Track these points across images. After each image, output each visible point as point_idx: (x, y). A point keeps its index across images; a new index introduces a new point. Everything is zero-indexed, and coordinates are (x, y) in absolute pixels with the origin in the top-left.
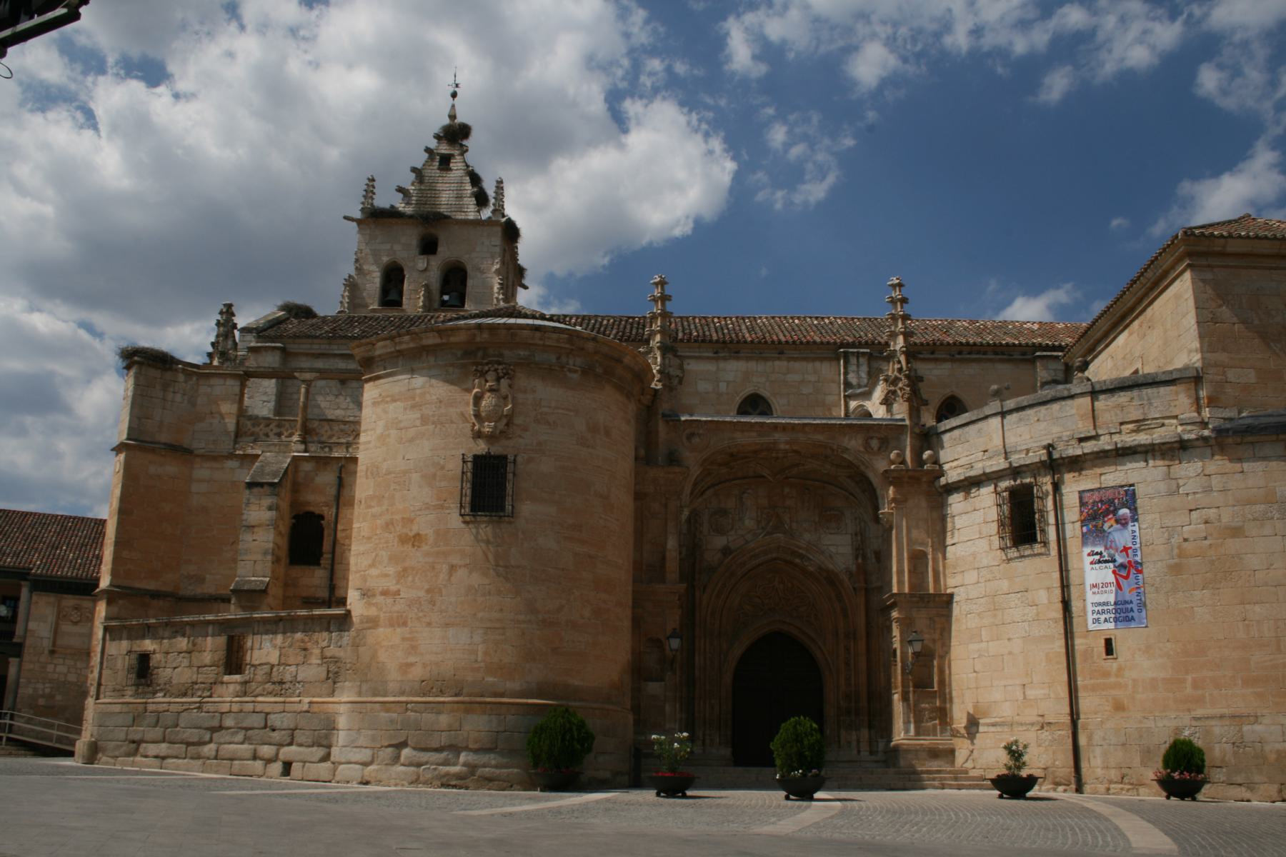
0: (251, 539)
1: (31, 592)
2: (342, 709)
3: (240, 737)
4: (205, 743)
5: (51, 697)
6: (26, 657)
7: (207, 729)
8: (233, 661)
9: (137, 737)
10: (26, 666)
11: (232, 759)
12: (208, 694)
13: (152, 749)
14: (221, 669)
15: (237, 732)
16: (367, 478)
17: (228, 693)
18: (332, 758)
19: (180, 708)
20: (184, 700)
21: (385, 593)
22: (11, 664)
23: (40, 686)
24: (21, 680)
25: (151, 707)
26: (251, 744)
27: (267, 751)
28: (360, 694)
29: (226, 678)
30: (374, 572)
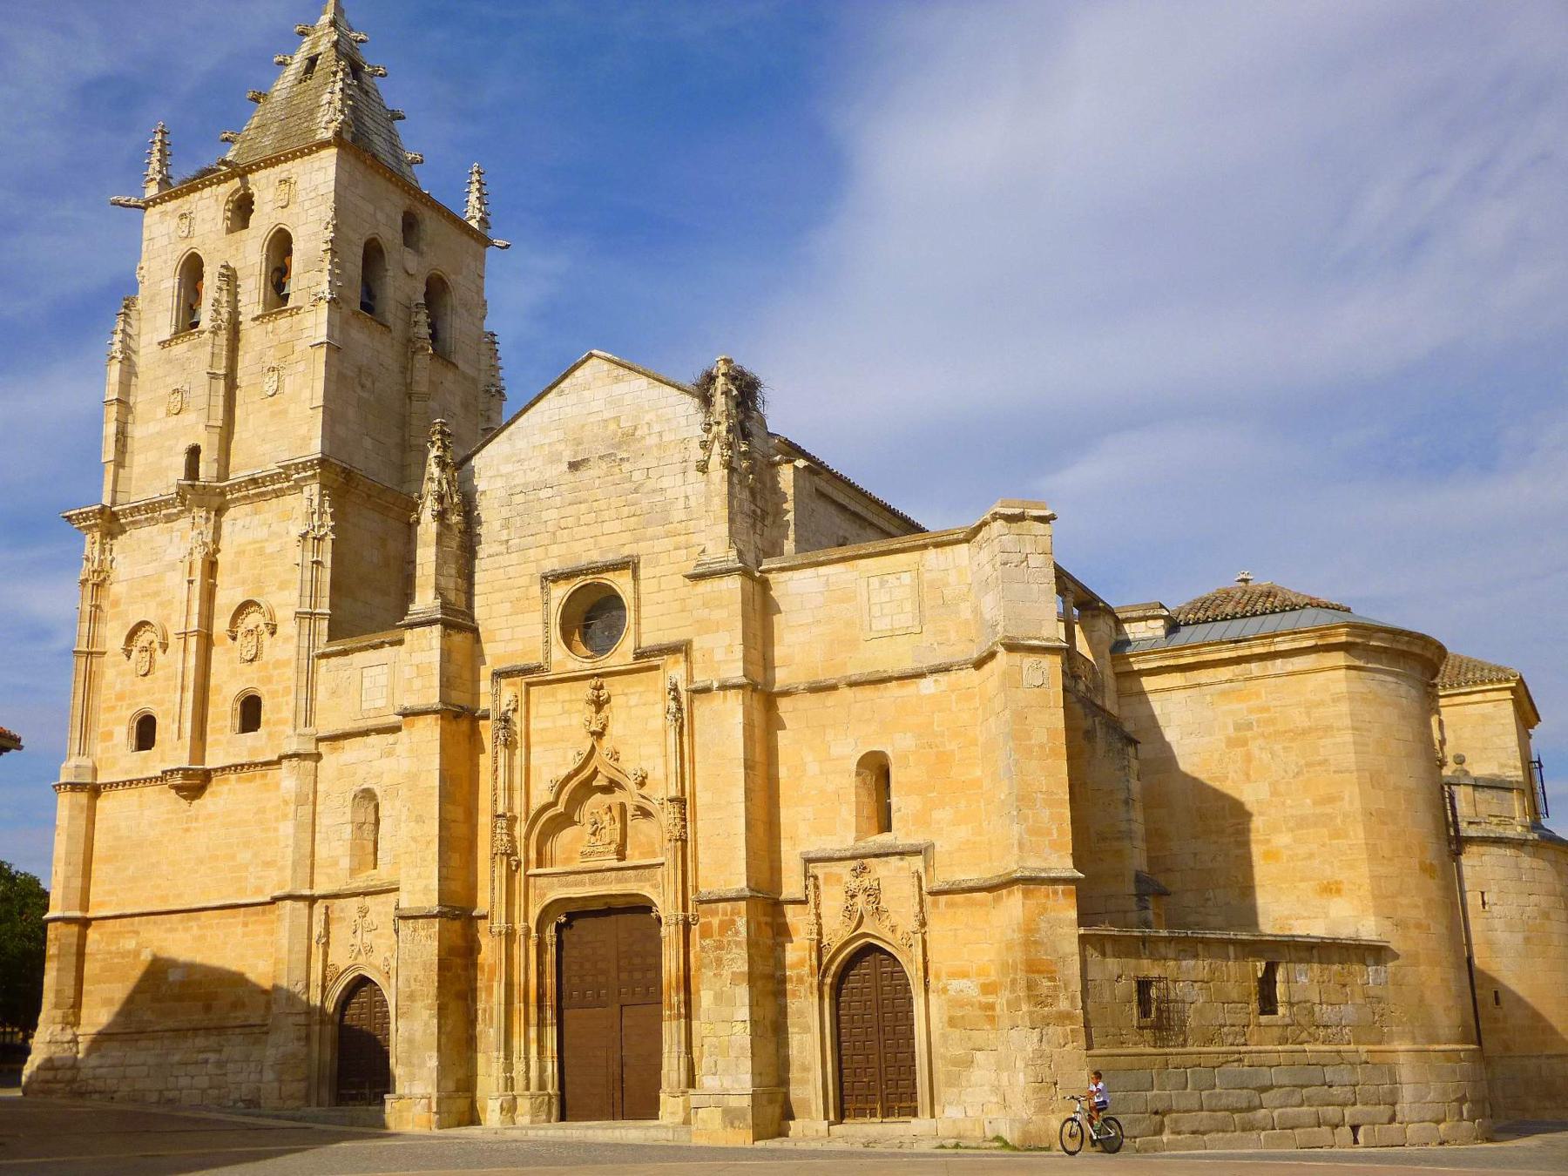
2: (1402, 1058)
4: (1255, 1109)
9: (1160, 1106)
16: (1373, 787)
17: (1265, 1044)
18: (1399, 1117)
19: (1215, 1061)
20: (1212, 1049)
21: (1418, 926)
25: (1173, 1061)
26: (1311, 1106)
27: (1331, 1112)
28: (1415, 1042)
29: (1264, 1019)
30: (1404, 901)
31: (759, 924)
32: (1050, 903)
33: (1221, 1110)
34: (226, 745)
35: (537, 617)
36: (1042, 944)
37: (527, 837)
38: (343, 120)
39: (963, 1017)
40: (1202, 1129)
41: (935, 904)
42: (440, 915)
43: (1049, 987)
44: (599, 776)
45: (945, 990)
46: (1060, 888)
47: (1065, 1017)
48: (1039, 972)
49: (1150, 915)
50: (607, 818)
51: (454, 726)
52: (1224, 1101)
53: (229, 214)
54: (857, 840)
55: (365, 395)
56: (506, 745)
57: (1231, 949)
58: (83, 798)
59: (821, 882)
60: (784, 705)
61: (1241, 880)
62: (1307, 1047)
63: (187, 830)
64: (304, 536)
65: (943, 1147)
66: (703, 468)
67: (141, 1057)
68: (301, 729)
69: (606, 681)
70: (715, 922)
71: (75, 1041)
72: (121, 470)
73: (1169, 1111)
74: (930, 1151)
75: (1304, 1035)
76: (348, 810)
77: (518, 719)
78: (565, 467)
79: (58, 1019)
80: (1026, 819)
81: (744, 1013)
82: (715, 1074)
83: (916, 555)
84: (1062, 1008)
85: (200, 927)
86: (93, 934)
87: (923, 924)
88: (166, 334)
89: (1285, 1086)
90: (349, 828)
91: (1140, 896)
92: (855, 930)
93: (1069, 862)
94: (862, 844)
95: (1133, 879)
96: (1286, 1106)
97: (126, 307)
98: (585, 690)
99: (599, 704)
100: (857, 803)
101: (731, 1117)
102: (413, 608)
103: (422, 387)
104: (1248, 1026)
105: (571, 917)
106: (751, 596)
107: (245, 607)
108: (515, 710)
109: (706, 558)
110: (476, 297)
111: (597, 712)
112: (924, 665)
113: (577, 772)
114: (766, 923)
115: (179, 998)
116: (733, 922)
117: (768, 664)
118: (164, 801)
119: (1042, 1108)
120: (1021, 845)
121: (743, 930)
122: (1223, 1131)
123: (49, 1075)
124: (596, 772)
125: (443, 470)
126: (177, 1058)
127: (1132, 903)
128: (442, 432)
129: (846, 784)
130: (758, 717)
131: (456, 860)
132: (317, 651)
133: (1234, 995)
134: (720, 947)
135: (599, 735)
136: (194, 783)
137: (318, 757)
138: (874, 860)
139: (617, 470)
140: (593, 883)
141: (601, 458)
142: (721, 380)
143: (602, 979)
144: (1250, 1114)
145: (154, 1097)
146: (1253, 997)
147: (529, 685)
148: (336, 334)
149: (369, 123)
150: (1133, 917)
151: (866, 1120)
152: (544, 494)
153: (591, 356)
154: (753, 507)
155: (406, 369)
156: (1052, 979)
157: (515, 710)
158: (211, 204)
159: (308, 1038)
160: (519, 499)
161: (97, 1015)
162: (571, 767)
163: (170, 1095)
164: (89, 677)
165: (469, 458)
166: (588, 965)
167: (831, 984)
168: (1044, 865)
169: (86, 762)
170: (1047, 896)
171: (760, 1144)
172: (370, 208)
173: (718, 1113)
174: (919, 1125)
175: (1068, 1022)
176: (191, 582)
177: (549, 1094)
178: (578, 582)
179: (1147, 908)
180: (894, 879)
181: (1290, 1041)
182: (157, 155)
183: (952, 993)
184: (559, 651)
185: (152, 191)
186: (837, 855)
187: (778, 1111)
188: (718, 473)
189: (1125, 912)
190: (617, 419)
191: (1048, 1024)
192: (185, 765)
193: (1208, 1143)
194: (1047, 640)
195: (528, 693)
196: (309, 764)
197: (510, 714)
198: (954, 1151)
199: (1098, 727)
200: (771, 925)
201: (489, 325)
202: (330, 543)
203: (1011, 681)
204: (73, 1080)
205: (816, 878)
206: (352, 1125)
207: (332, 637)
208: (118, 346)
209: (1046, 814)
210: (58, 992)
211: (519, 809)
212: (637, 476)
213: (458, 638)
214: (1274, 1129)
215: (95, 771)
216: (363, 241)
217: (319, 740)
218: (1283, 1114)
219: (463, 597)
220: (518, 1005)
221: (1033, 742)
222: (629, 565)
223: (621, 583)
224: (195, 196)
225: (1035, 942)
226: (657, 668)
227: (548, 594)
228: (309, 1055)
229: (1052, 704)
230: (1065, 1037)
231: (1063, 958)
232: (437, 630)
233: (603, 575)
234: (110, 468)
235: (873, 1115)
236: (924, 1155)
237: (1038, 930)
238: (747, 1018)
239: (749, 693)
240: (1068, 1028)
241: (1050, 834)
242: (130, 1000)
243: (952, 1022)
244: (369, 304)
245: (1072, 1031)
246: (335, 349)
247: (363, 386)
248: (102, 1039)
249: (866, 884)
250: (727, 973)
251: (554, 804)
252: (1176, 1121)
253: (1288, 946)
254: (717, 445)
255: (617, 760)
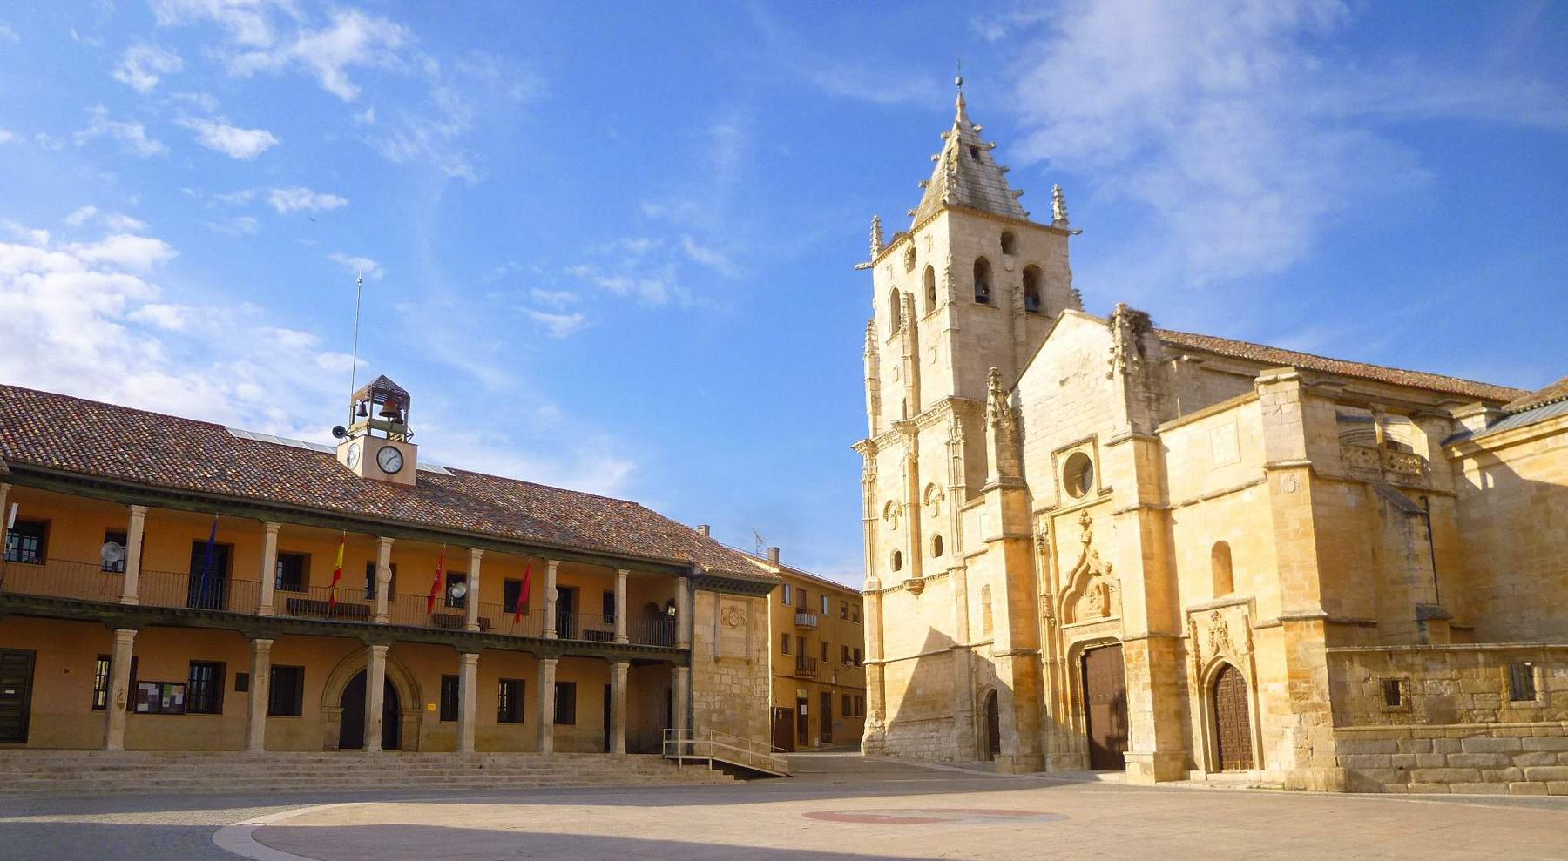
0: (1418, 568)
1: (691, 592)
3: (1551, 758)
4: (1504, 767)
5: (721, 712)
6: (696, 667)
7: (1527, 752)
8: (1521, 690)
9: (1404, 765)
10: (697, 677)
11: (1545, 781)
12: (1493, 719)
13: (1430, 775)
14: (1505, 694)
15: (1547, 755)
17: (1517, 721)
19: (1461, 734)
22: (681, 674)
23: (711, 699)
24: (695, 693)
29: (1514, 704)
31: (1161, 653)
32: (1304, 633)
33: (1467, 768)
34: (931, 565)
35: (1051, 477)
36: (1300, 659)
37: (1059, 607)
38: (950, 194)
39: (1276, 707)
40: (1446, 779)
41: (1258, 635)
42: (1012, 654)
43: (1305, 688)
44: (1091, 569)
45: (1266, 690)
46: (1312, 623)
47: (1315, 707)
48: (1297, 678)
49: (1428, 634)
50: (1096, 592)
51: (1015, 546)
52: (1469, 761)
53: (907, 262)
54: (1215, 598)
55: (984, 352)
56: (1042, 553)
57: (1481, 657)
58: (874, 599)
59: (1197, 625)
60: (1175, 514)
61: (1547, 602)
62: (1563, 723)
63: (918, 613)
64: (948, 444)
65: (1251, 787)
66: (1111, 376)
67: (908, 734)
68: (956, 554)
69: (1088, 510)
70: (1133, 652)
71: (883, 726)
72: (878, 417)
73: (1414, 767)
74: (1245, 790)
75: (1562, 715)
76: (980, 597)
77: (1049, 537)
78: (1058, 384)
79: (874, 715)
80: (1286, 580)
81: (1149, 707)
82: (1138, 743)
83: (1234, 411)
84: (1315, 701)
85: (927, 665)
86: (886, 669)
87: (1251, 648)
88: (888, 335)
89: (1536, 751)
90: (981, 607)
91: (1420, 621)
92: (1215, 654)
93: (1318, 606)
94: (1217, 600)
95: (1415, 609)
96: (1539, 765)
97: (870, 325)
98: (1078, 515)
99: (1086, 525)
100: (1214, 574)
101: (1144, 767)
102: (988, 480)
103: (1022, 339)
104: (1499, 709)
105: (1088, 652)
106: (1145, 452)
107: (930, 486)
108: (1047, 533)
109: (1116, 433)
110: (1063, 270)
111: (1086, 529)
112: (1243, 483)
113: (1080, 566)
114: (1169, 652)
115: (923, 704)
116: (1141, 653)
117: (1163, 490)
118: (906, 596)
119: (1302, 764)
120: (1282, 597)
121: (1148, 659)
122: (1468, 781)
123: (871, 744)
124: (1088, 567)
125: (996, 397)
126: (922, 735)
127: (1415, 627)
128: (995, 375)
129: (1206, 560)
130: (1155, 526)
131: (1022, 622)
132: (960, 509)
133: (1484, 687)
134: (1136, 668)
135: (1088, 543)
136: (918, 587)
137: (966, 568)
138: (1222, 609)
139: (1081, 382)
140: (1092, 631)
141: (1074, 375)
142: (1118, 319)
143: (1106, 687)
144: (1497, 771)
145: (914, 755)
146: (1504, 689)
147: (1053, 517)
148: (956, 322)
149: (984, 182)
150: (1417, 636)
151: (1233, 771)
152: (1051, 401)
153: (1064, 313)
154: (1147, 394)
155: (1012, 329)
156: (1307, 682)
157: (1047, 533)
158: (898, 256)
159: (972, 724)
160: (1039, 407)
161: (892, 713)
162: (1075, 565)
163: (920, 754)
164: (872, 532)
165: (1016, 384)
166: (1099, 680)
167: (1208, 688)
168: (1299, 609)
169: (875, 579)
170: (1302, 629)
171: (1159, 783)
172: (975, 239)
173: (1138, 765)
174: (1252, 775)
175: (1319, 710)
176: (905, 476)
177: (1081, 755)
178: (1070, 452)
179: (1424, 630)
180: (1234, 619)
181: (1545, 719)
182: (875, 235)
183: (1270, 692)
184: (1065, 495)
185: (875, 256)
186: (1202, 608)
187: (1179, 764)
188: (1119, 378)
189: (1411, 633)
190: (1080, 350)
191: (1305, 711)
192: (910, 578)
193: (1453, 790)
194: (1298, 460)
195: (1053, 522)
196: (961, 572)
197: (1044, 536)
198: (1256, 790)
199: (1387, 507)
200: (1174, 654)
201: (1074, 286)
202: (962, 445)
203: (1275, 492)
204: (882, 748)
205: (1194, 623)
206: (983, 771)
207: (967, 500)
208: (867, 349)
209: (1300, 575)
210: (873, 701)
211: (1053, 591)
212: (1092, 384)
213: (1013, 495)
214: (1524, 780)
215: (880, 583)
216: (974, 259)
217: (965, 559)
218: (1533, 771)
219: (1016, 470)
220: (1062, 705)
221: (1289, 529)
222: (1092, 440)
223: (1088, 450)
224: (892, 254)
225: (1295, 659)
226: (1109, 500)
227: (1056, 461)
228: (973, 736)
229: (1302, 502)
230: (1318, 719)
231: (1315, 669)
232: (998, 491)
233: (1080, 447)
234: (871, 417)
235: (1236, 768)
236: (1242, 792)
237: (1296, 651)
238: (1151, 710)
239: (1145, 512)
240: (1320, 714)
241: (1303, 587)
242: (903, 705)
243: (1271, 710)
244: (983, 299)
245: (1322, 715)
246: (955, 332)
247: (983, 347)
248: (894, 724)
249: (1219, 625)
250: (1141, 686)
251: (1070, 586)
252: (1420, 774)
253: (1543, 650)
254: (1117, 360)
255: (1097, 558)
